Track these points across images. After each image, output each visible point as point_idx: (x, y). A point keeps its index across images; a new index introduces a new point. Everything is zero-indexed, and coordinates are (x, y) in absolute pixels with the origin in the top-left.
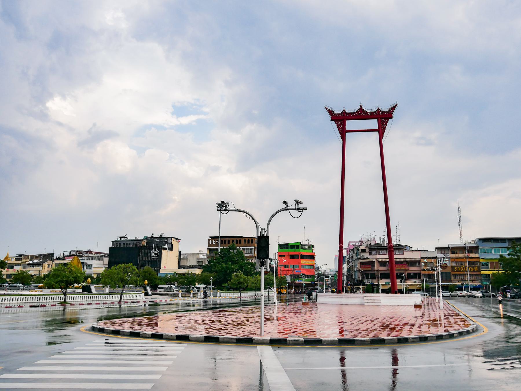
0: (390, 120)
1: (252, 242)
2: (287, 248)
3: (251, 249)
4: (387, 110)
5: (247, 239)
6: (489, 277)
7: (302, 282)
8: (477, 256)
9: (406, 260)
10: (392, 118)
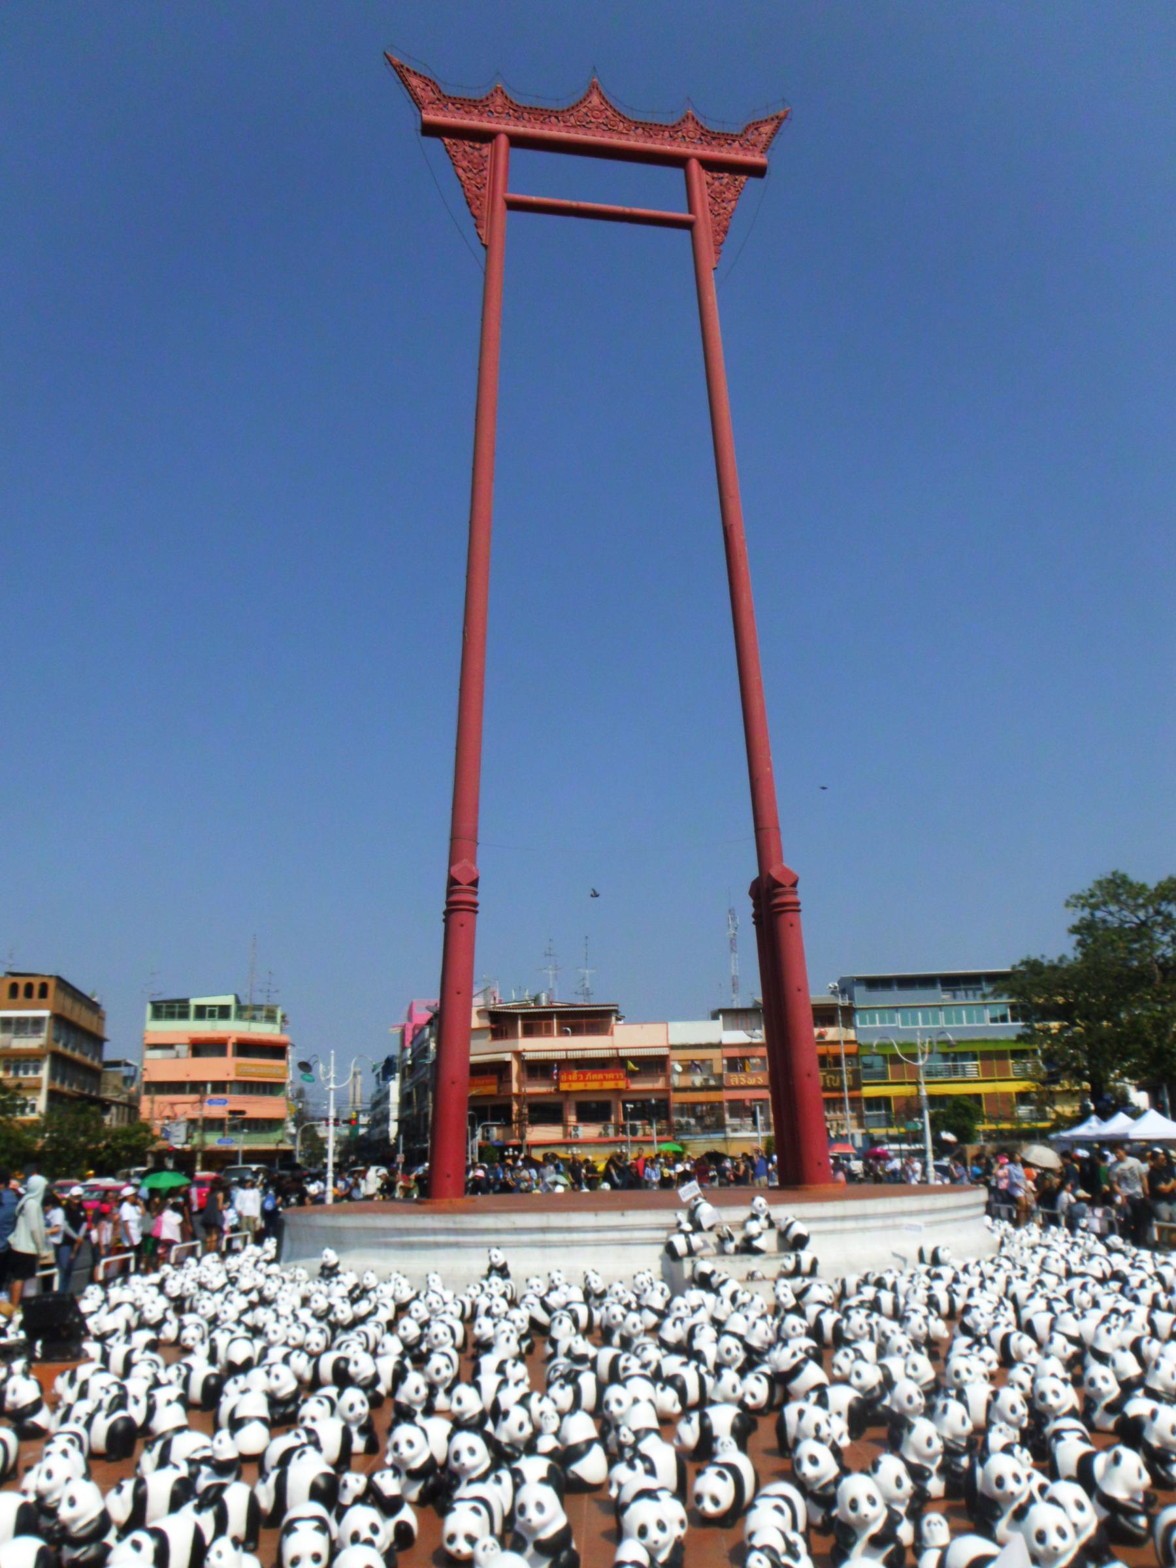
0: (753, 181)
1: (43, 993)
2: (184, 1015)
3: (38, 1022)
4: (737, 131)
5: (22, 982)
6: (888, 1107)
7: (235, 1147)
8: (851, 1034)
9: (623, 1053)
10: (757, 171)
